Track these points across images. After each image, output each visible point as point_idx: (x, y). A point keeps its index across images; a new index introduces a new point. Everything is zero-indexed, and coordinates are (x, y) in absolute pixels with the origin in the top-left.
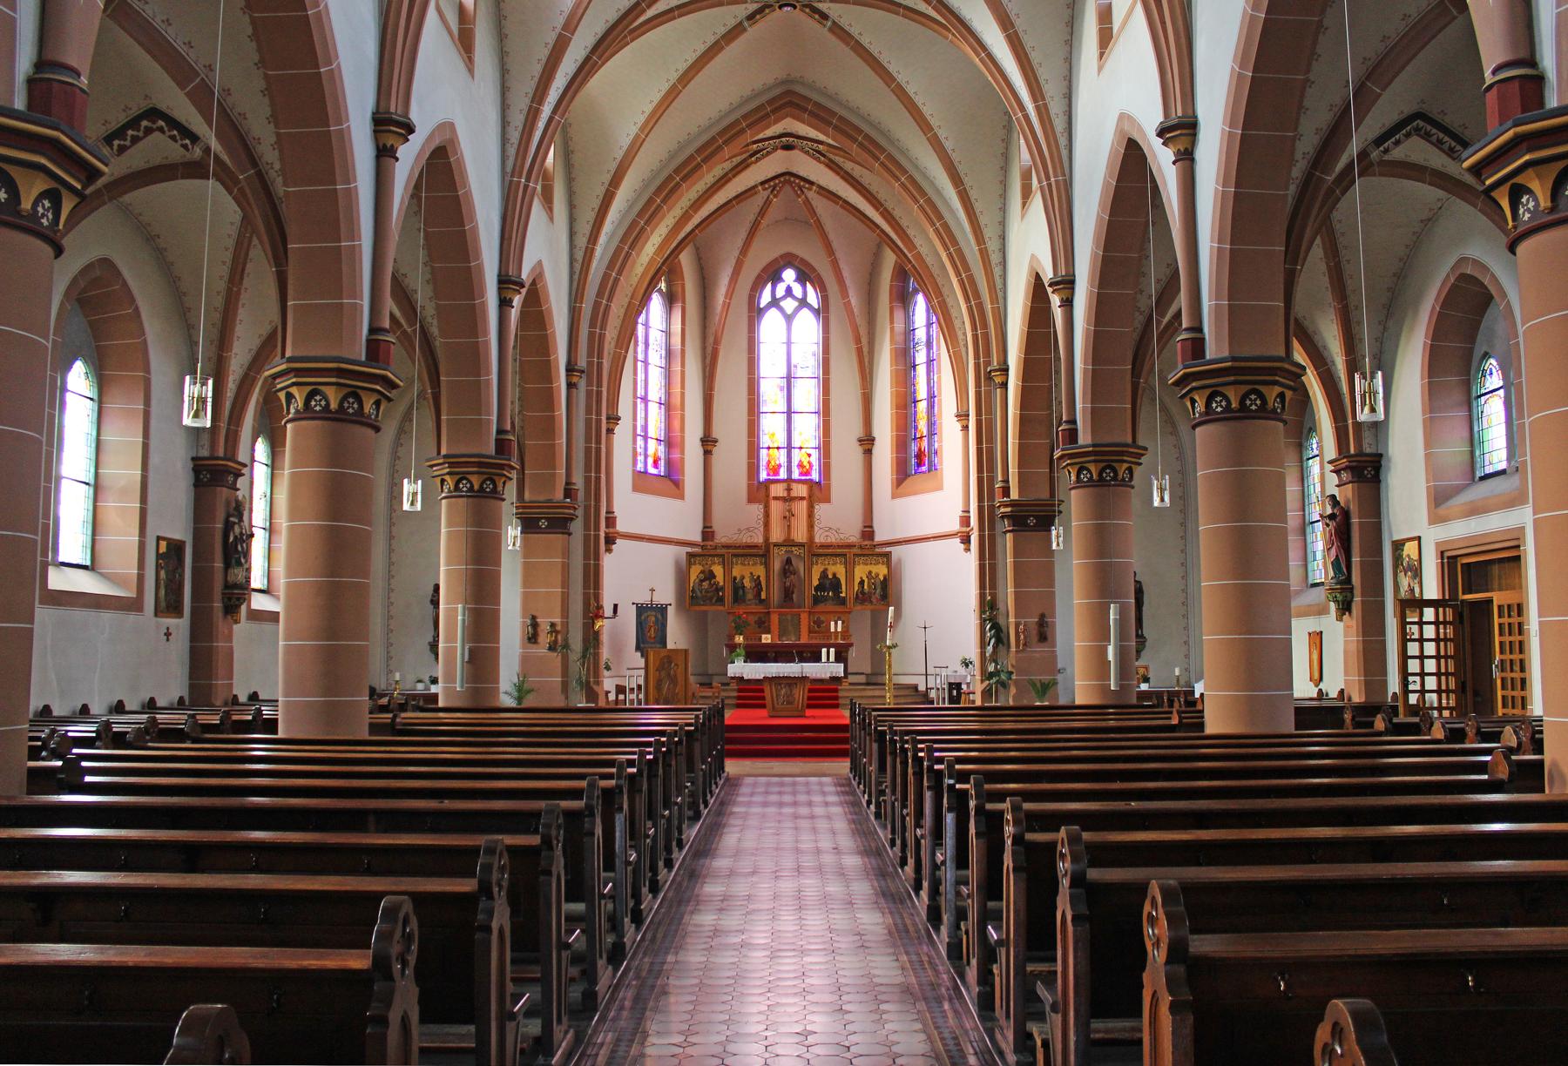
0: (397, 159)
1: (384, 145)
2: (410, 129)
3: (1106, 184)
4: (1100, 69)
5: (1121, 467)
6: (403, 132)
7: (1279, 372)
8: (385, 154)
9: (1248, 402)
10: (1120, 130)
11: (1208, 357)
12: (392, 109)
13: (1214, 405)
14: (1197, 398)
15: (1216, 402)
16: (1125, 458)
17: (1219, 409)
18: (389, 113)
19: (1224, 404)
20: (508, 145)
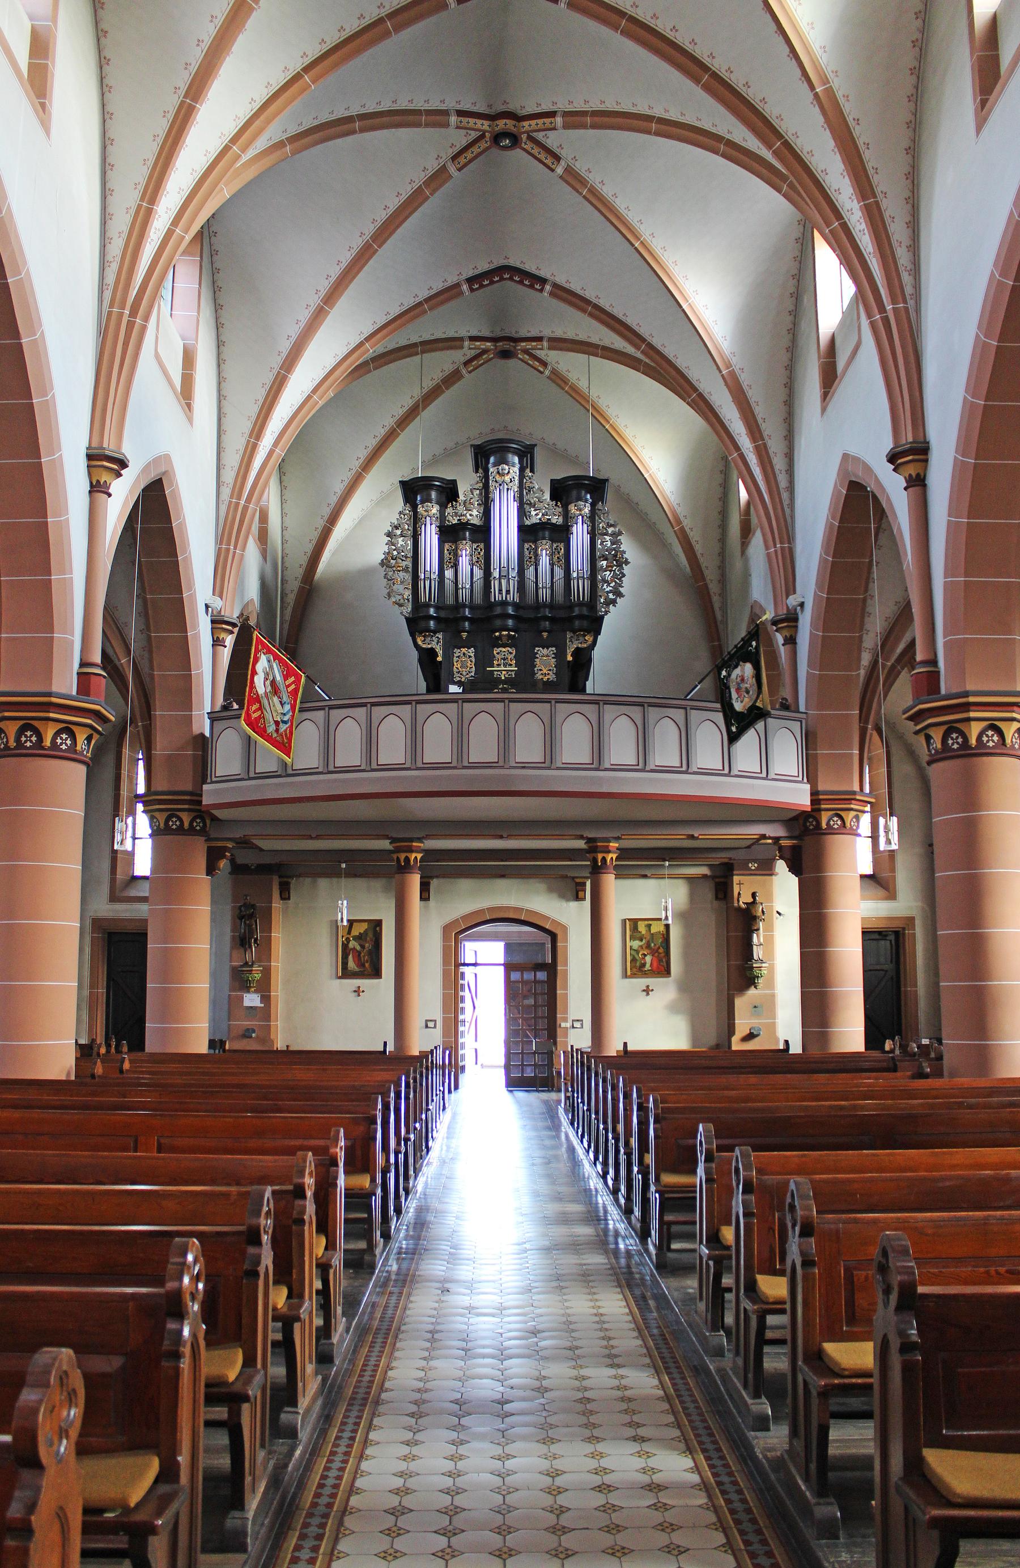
0: (110, 495)
1: (98, 482)
2: (123, 464)
3: (829, 526)
4: (824, 410)
5: (848, 816)
6: (115, 467)
7: (1015, 708)
8: (97, 489)
9: (985, 739)
10: (843, 470)
11: (943, 692)
12: (105, 445)
13: (950, 742)
14: (932, 734)
15: (952, 739)
16: (852, 806)
17: (955, 746)
18: (104, 449)
19: (960, 740)
20: (222, 488)
